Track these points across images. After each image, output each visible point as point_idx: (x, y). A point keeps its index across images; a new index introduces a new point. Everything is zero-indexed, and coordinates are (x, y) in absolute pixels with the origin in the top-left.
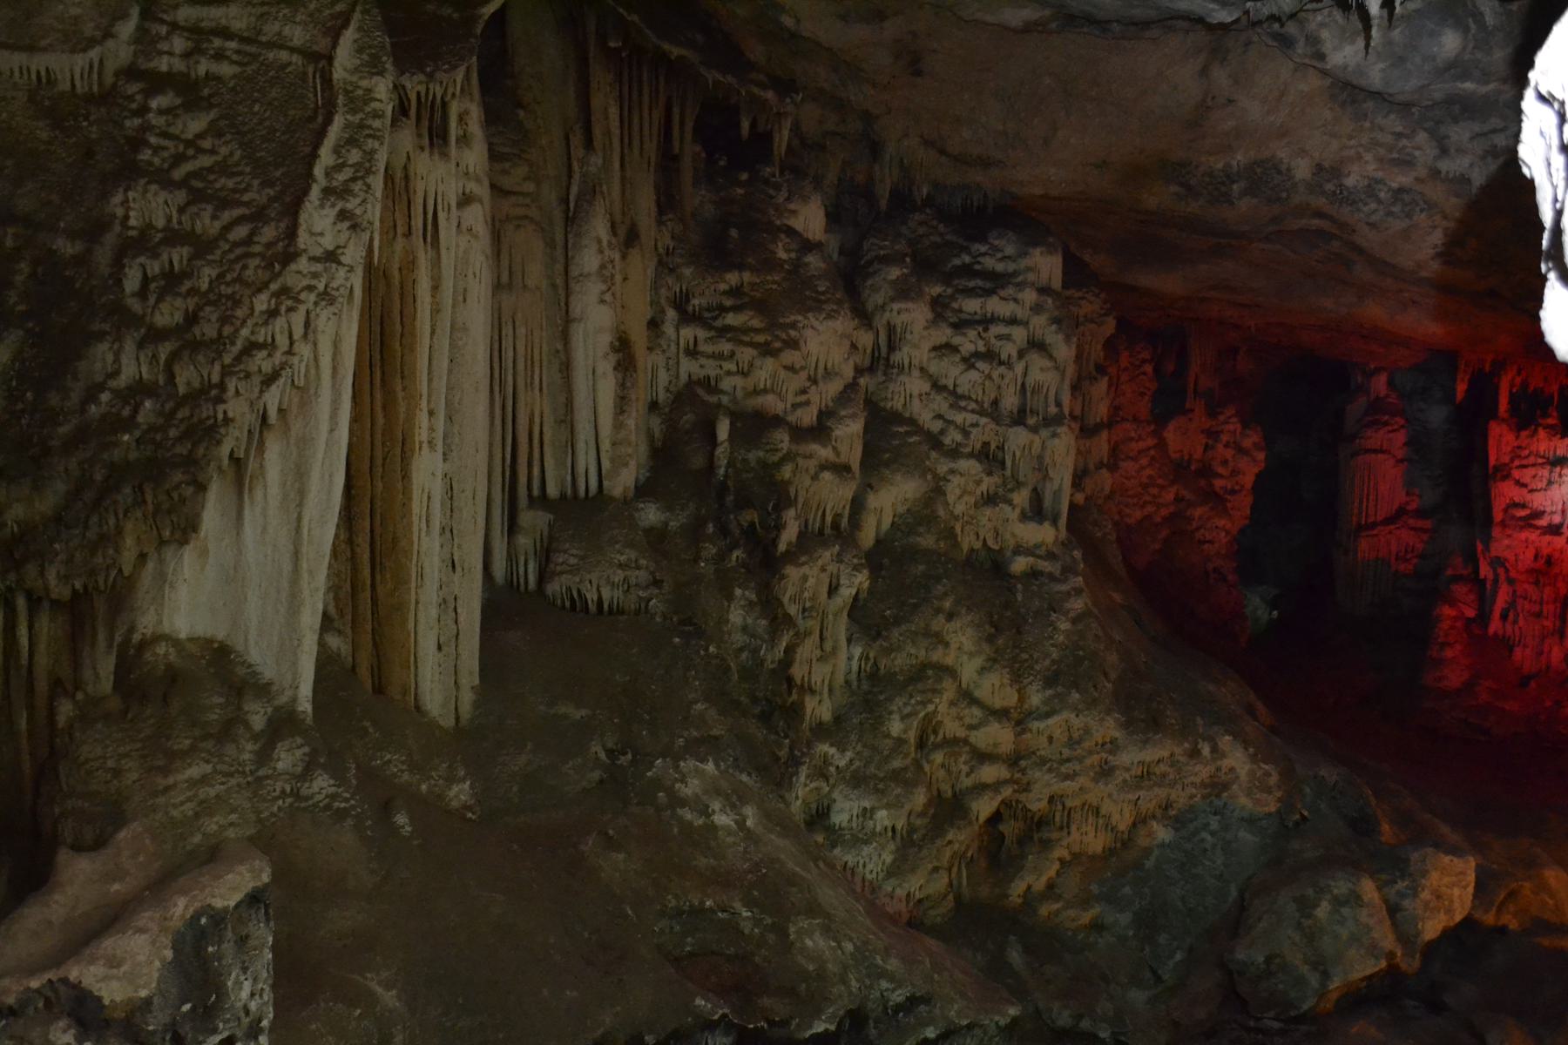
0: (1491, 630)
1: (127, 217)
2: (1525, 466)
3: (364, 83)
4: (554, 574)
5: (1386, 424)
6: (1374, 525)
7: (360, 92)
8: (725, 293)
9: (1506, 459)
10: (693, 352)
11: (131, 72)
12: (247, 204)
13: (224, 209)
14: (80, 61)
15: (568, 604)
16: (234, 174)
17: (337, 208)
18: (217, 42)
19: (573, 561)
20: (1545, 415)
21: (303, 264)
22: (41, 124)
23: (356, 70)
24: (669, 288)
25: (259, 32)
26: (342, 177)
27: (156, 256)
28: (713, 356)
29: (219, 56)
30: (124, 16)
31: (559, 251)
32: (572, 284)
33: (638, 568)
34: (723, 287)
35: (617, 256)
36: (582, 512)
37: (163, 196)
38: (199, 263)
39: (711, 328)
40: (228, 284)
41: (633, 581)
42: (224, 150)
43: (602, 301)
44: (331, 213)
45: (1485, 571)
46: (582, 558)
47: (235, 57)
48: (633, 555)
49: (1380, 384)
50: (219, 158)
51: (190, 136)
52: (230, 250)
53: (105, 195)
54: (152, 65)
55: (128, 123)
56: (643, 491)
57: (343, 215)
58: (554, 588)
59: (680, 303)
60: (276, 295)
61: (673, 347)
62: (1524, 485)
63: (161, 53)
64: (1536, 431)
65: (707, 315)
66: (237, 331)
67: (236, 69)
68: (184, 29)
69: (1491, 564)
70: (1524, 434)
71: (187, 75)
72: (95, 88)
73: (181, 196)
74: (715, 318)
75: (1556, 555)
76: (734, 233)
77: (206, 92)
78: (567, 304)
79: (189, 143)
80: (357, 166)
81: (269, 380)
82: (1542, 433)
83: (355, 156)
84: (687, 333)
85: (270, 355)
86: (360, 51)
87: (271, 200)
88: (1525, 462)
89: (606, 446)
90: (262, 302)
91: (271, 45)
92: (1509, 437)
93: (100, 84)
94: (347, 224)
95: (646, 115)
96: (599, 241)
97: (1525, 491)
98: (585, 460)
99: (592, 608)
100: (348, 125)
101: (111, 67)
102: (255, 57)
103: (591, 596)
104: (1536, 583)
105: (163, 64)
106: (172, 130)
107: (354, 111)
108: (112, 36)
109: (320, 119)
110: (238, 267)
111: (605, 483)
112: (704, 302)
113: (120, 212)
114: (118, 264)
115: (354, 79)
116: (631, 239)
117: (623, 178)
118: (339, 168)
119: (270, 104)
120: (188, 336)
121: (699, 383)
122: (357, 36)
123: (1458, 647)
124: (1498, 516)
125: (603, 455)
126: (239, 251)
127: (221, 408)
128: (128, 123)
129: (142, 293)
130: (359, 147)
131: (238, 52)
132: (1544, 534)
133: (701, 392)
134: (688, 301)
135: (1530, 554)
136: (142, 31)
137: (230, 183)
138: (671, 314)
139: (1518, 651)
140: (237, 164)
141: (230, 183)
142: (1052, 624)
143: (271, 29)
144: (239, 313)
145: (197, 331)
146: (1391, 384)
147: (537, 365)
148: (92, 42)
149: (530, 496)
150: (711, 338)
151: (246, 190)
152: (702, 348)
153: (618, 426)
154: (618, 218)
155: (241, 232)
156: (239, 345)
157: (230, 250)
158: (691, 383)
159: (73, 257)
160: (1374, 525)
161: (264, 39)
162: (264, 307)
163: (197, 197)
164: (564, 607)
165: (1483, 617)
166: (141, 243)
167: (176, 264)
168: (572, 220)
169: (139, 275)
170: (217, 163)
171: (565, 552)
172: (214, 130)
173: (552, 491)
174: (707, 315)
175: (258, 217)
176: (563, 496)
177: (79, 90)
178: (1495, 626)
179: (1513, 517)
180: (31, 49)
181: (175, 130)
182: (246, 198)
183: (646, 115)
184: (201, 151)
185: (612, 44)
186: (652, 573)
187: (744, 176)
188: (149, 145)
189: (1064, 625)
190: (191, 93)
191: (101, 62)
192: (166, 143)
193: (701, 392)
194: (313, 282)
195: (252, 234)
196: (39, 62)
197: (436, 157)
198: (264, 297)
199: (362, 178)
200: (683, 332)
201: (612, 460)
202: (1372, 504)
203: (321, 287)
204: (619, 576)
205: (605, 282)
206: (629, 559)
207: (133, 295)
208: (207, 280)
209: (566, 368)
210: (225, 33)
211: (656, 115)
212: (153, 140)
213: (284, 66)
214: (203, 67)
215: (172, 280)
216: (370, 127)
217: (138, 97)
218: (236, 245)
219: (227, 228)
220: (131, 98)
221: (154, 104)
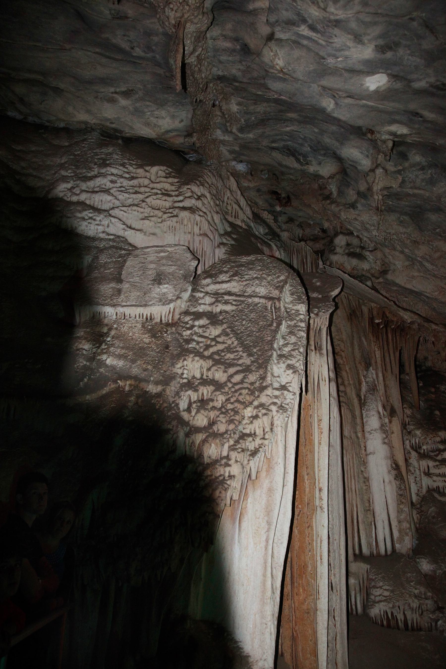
1: (183, 374)
3: (295, 308)
4: (375, 602)
7: (293, 312)
8: (439, 442)
10: (428, 474)
11: (186, 313)
12: (240, 365)
13: (229, 367)
15: (385, 623)
16: (234, 352)
17: (286, 364)
18: (226, 297)
19: (386, 593)
21: (269, 391)
22: (146, 336)
23: (292, 302)
24: (410, 441)
26: (287, 349)
27: (196, 391)
28: (439, 475)
29: (226, 303)
30: (186, 290)
31: (358, 421)
32: (367, 435)
33: (426, 599)
34: (438, 439)
35: (387, 420)
36: (385, 563)
38: (218, 393)
39: (436, 460)
40: (232, 403)
41: (424, 607)
42: (229, 342)
43: (385, 443)
44: (283, 366)
46: (392, 591)
47: (234, 303)
48: (423, 590)
50: (226, 345)
51: (213, 337)
52: (233, 387)
53: (173, 365)
54: (196, 310)
55: (184, 333)
56: (417, 551)
57: (289, 367)
58: (375, 611)
59: (416, 448)
60: (256, 407)
61: (417, 471)
63: (200, 304)
65: (432, 454)
66: (237, 426)
67: (234, 308)
71: (212, 312)
72: (170, 321)
73: (210, 362)
74: (437, 455)
76: (437, 412)
77: (221, 318)
78: (365, 447)
79: (212, 340)
80: (295, 344)
81: (254, 453)
83: (293, 339)
84: (424, 463)
85: (253, 440)
86: (292, 294)
89: (394, 524)
90: (249, 412)
91: (250, 296)
93: (172, 320)
94: (291, 371)
95: (392, 355)
96: (379, 413)
98: (382, 532)
99: (401, 625)
100: (289, 326)
101: (177, 312)
102: (243, 302)
103: (400, 617)
105: (201, 309)
106: (205, 334)
107: (291, 320)
108: (181, 298)
109: (275, 325)
110: (237, 394)
111: (397, 546)
112: (429, 447)
113: (180, 371)
114: (177, 394)
115: (290, 306)
116: (392, 413)
117: (385, 384)
118: (286, 345)
119: (250, 320)
120: (211, 431)
121: (434, 490)
122: (290, 288)
125: (393, 527)
126: (237, 387)
127: (227, 469)
128: (184, 333)
129: (188, 410)
130: (295, 335)
131: (235, 301)
133: (436, 495)
134: (420, 448)
136: (192, 296)
137: (232, 356)
138: (414, 454)
140: (236, 347)
141: (232, 356)
143: (249, 291)
144: (237, 417)
145: (215, 428)
147: (353, 478)
148: (171, 301)
149: (355, 555)
150: (437, 466)
152: (432, 471)
153: (400, 511)
154: (385, 404)
155: (237, 378)
156: (237, 436)
157: (233, 387)
158: (430, 491)
159: (156, 394)
162: (250, 415)
163: (217, 362)
164: (382, 625)
166: (190, 385)
167: (205, 395)
168: (362, 404)
169: (187, 401)
171: (381, 587)
172: (224, 333)
173: (365, 550)
174: (432, 454)
175: (247, 370)
176: (372, 554)
177: (163, 322)
180: (145, 305)
181: (206, 334)
182: (240, 362)
183: (392, 355)
184: (218, 342)
185: (377, 321)
186: (435, 602)
187: (433, 390)
188: (194, 340)
191: (174, 309)
193: (436, 495)
194: (275, 400)
195: (244, 378)
197: (318, 355)
198: (249, 409)
199: (298, 349)
200: (421, 462)
201: (400, 531)
203: (279, 403)
204: (415, 604)
205: (384, 433)
206: (420, 592)
207: (184, 411)
208: (220, 402)
209: (367, 480)
210: (229, 293)
211: (397, 354)
212: (196, 338)
213: (256, 305)
214: (220, 308)
215: (203, 403)
216: (299, 326)
217: (190, 322)
219: (232, 376)
220: (187, 323)
221: (197, 323)
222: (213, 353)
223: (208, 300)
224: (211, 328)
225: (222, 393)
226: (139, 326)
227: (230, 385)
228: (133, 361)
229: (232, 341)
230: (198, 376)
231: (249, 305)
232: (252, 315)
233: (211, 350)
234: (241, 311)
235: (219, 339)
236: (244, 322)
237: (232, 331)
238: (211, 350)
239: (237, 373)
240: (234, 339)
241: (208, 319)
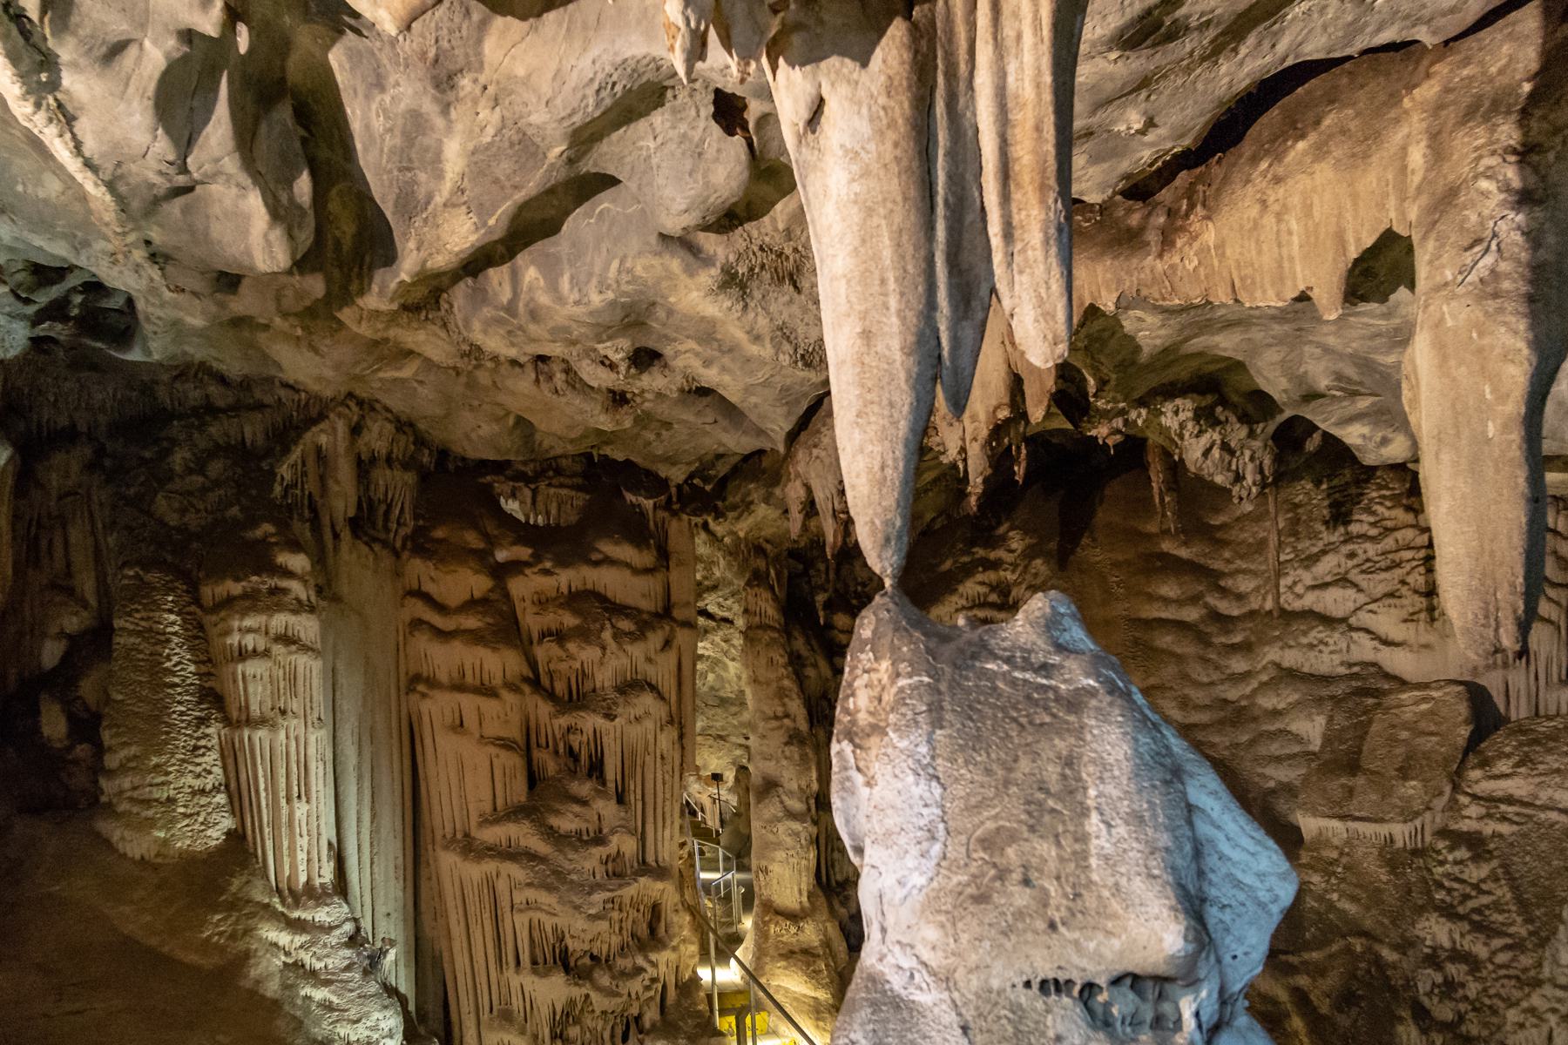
12: (1510, 935)
14: (1407, 828)
16: (1504, 911)
18: (1503, 807)
25: (1536, 797)
29: (1504, 818)
30: (1441, 794)
37: (1449, 924)
40: (1490, 997)
42: (1499, 893)
47: (1516, 819)
51: (1474, 881)
60: (1525, 1011)
68: (1480, 798)
77: (1492, 846)
79: (1476, 887)
87: (1531, 934)
90: (1513, 1015)
91: (1544, 808)
102: (1530, 817)
105: (1465, 826)
113: (1421, 934)
131: (1518, 814)
137: (1500, 918)
141: (1500, 918)
143: (1544, 796)
148: (1417, 814)
151: (1511, 924)
155: (1502, 958)
161: (1538, 803)
163: (1478, 927)
166: (1433, 960)
170: (1494, 902)
175: (1517, 946)
180: (1381, 821)
181: (1465, 876)
182: (1512, 930)
190: (1476, 844)
192: (1456, 885)
194: (1557, 1006)
195: (1514, 959)
196: (1383, 830)
210: (1510, 800)
212: (1447, 884)
213: (1552, 825)
214: (1489, 828)
218: (1500, 967)
219: (1494, 953)
220: (1439, 852)
222: (1474, 910)
223: (1474, 810)
224: (1472, 866)
225: (1476, 979)
226: (1375, 852)
227: (1490, 967)
228: (1368, 909)
229: (1503, 892)
230: (1447, 944)
231: (1539, 825)
232: (1544, 846)
233: (1471, 904)
234: (1525, 835)
235: (1484, 887)
236: (1528, 858)
237: (1507, 872)
238: (1471, 904)
239: (1507, 947)
240: (1506, 889)
241: (1469, 848)
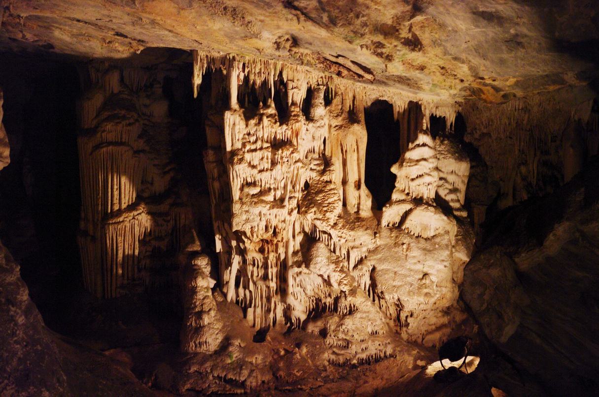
0: (229, 299)
2: (255, 150)
5: (124, 117)
6: (120, 212)
9: (238, 145)
20: (266, 106)
45: (219, 247)
49: (113, 81)
62: (254, 167)
64: (261, 120)
69: (226, 242)
70: (252, 122)
75: (280, 226)
82: (265, 119)
88: (253, 147)
92: (241, 124)
97: (255, 171)
104: (261, 251)
123: (213, 313)
124: (236, 194)
132: (273, 207)
135: (263, 224)
139: (250, 311)
142: (12, 319)
146: (122, 80)
160: (120, 212)
165: (220, 286)
178: (231, 295)
179: (248, 195)
189: (21, 320)
202: (116, 193)
